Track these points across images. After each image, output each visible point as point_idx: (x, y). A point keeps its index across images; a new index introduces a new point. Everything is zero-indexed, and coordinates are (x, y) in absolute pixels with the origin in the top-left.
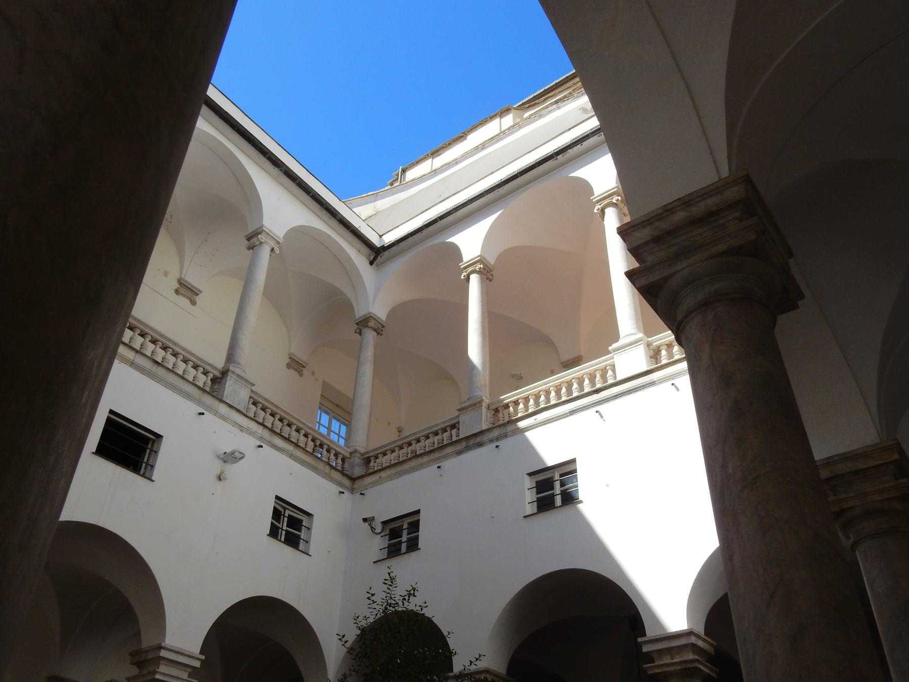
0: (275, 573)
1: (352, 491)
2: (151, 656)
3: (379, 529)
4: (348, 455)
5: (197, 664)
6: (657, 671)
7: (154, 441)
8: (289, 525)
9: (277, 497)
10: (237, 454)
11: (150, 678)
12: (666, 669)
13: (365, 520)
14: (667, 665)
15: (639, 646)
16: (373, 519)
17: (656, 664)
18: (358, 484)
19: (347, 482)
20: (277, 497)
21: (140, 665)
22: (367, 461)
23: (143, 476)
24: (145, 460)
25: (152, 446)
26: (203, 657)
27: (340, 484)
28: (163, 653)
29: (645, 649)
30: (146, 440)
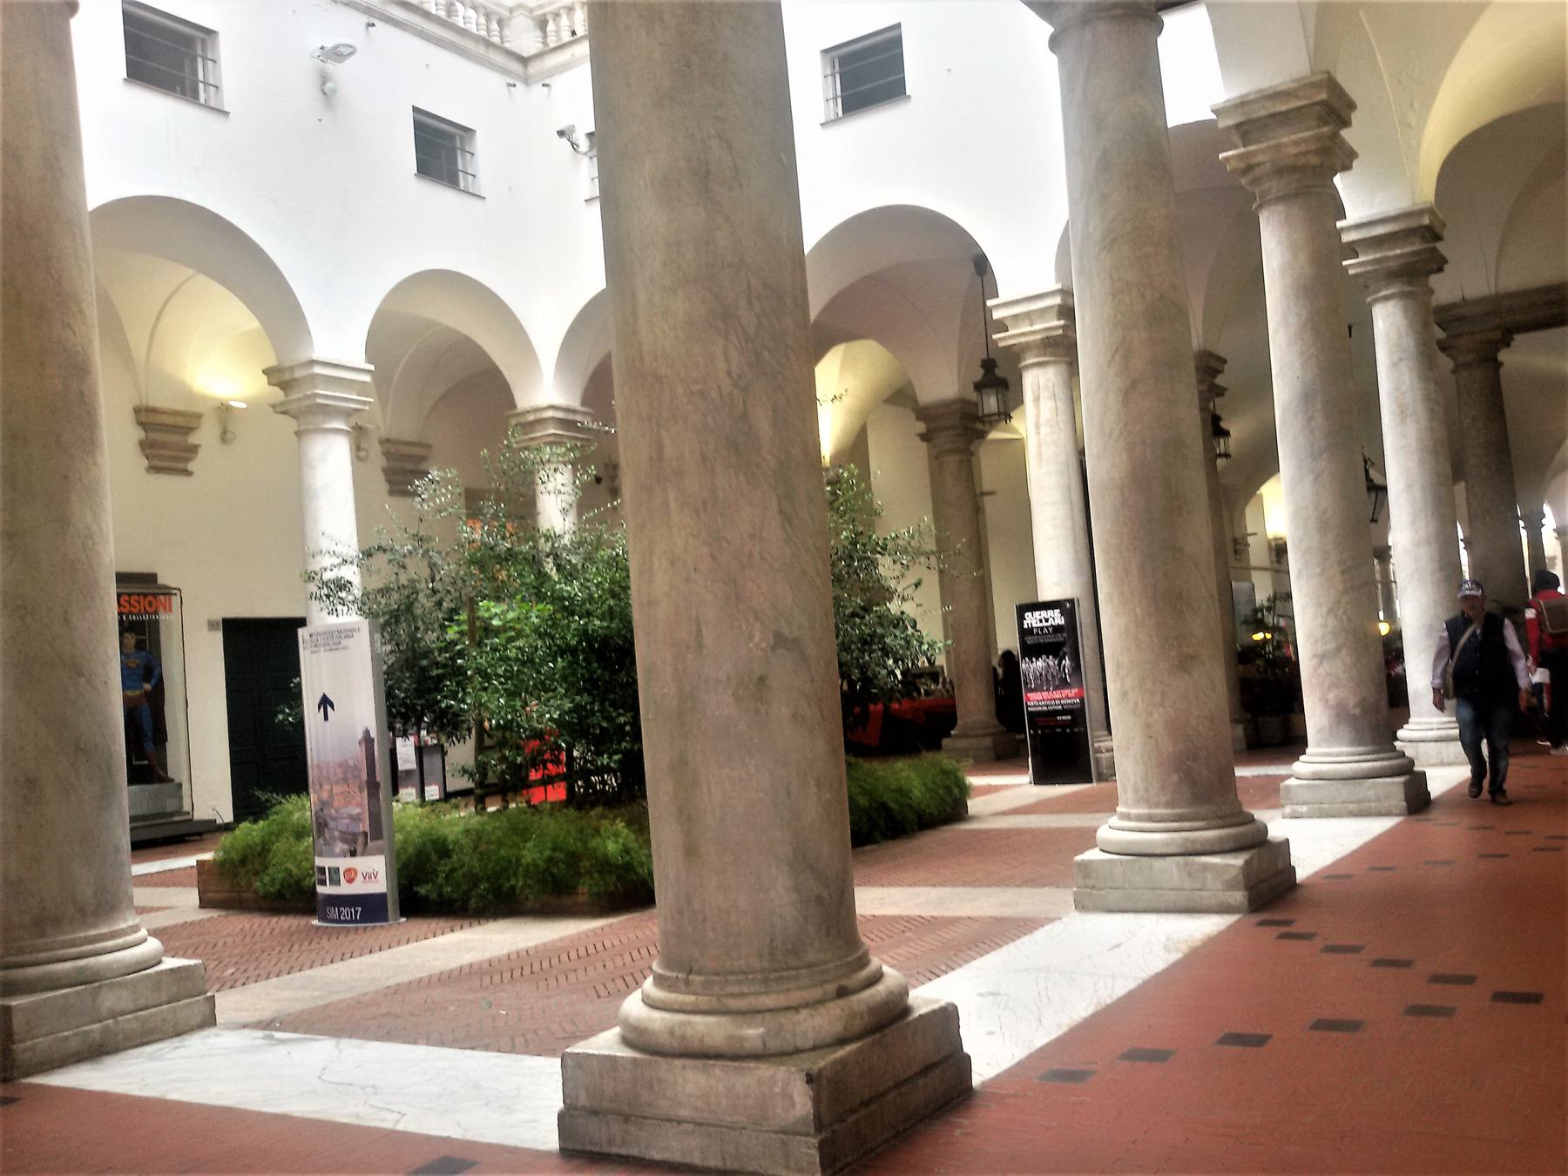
0: (436, 232)
1: (527, 81)
2: (298, 374)
3: (584, 144)
4: (506, 13)
5: (367, 378)
6: (1011, 342)
7: (204, 41)
8: (439, 149)
9: (415, 109)
10: (342, 49)
11: (307, 402)
12: (1023, 340)
13: (561, 133)
14: (1024, 334)
15: (987, 312)
16: (572, 129)
17: (1011, 332)
18: (534, 68)
19: (516, 67)
20: (415, 109)
21: (285, 386)
22: (542, 24)
23: (207, 107)
24: (201, 77)
25: (204, 49)
26: (372, 367)
27: (505, 71)
28: (318, 370)
29: (997, 315)
30: (188, 41)
